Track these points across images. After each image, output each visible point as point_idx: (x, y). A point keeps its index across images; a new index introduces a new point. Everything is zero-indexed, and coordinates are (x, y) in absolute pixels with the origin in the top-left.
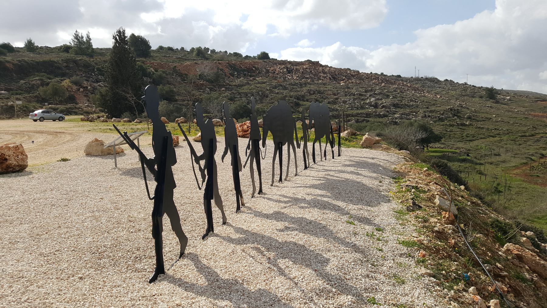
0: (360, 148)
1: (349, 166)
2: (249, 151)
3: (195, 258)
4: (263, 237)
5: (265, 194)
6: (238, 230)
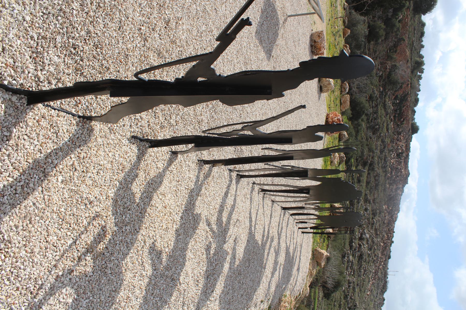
0: (313, 248)
1: (287, 253)
2: (290, 168)
3: (80, 140)
4: (136, 231)
5: (237, 182)
6: (154, 185)
